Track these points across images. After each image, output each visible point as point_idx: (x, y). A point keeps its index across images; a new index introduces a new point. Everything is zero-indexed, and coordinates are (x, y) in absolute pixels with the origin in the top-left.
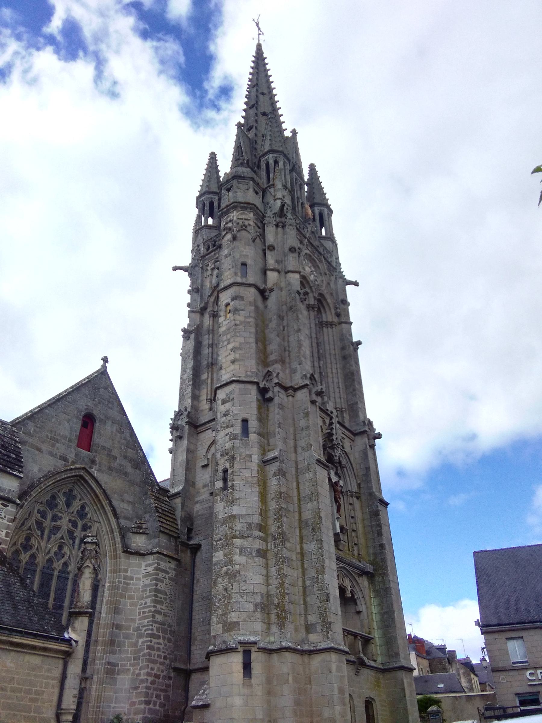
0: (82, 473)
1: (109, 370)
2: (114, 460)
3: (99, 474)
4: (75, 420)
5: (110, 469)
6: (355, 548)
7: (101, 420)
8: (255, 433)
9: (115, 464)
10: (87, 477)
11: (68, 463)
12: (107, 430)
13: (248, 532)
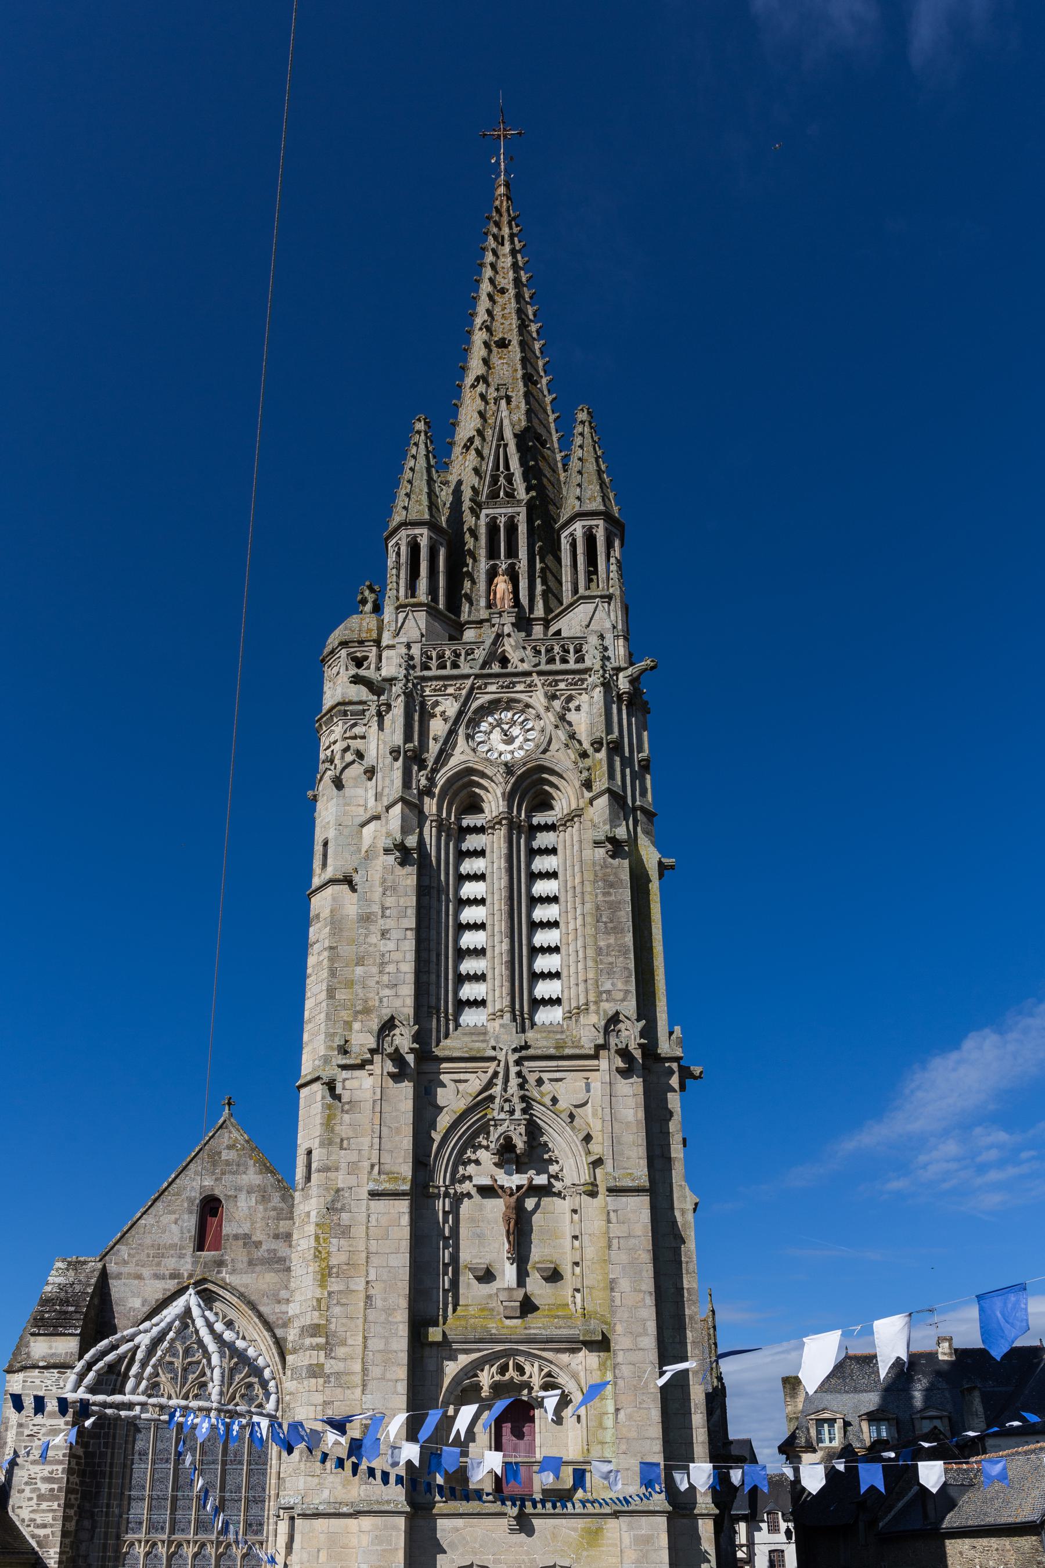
2: (257, 1247)
4: (186, 1216)
5: (251, 1263)
6: (578, 1296)
7: (228, 1197)
9: (261, 1253)
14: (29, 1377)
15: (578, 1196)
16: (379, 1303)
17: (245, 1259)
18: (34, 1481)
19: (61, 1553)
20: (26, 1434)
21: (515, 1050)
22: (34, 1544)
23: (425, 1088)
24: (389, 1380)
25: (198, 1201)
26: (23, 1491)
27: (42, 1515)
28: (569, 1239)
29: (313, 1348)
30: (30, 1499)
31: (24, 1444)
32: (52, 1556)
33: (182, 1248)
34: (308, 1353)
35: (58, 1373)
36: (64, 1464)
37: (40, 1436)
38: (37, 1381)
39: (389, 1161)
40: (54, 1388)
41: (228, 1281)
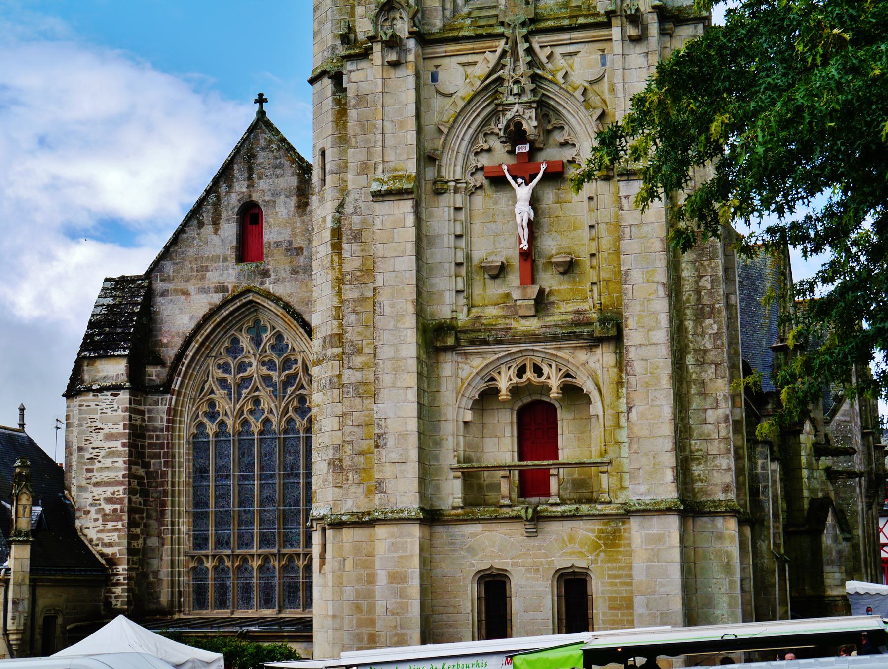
0: (251, 297)
1: (269, 116)
3: (276, 288)
5: (294, 272)
8: (332, 173)
10: (259, 299)
11: (228, 292)
12: (279, 214)
13: (324, 352)
14: (84, 401)
15: (595, 183)
16: (387, 310)
17: (288, 268)
18: (98, 502)
19: (129, 570)
20: (86, 457)
21: (523, 24)
22: (103, 562)
23: (433, 74)
24: (399, 388)
25: (236, 210)
26: (89, 512)
27: (108, 534)
28: (587, 228)
29: (334, 357)
30: (96, 520)
31: (85, 467)
32: (121, 572)
33: (225, 259)
34: (330, 363)
35: (112, 395)
36: (124, 485)
37: (100, 458)
38: (93, 405)
39: (393, 158)
40: (109, 411)
41: (272, 291)
